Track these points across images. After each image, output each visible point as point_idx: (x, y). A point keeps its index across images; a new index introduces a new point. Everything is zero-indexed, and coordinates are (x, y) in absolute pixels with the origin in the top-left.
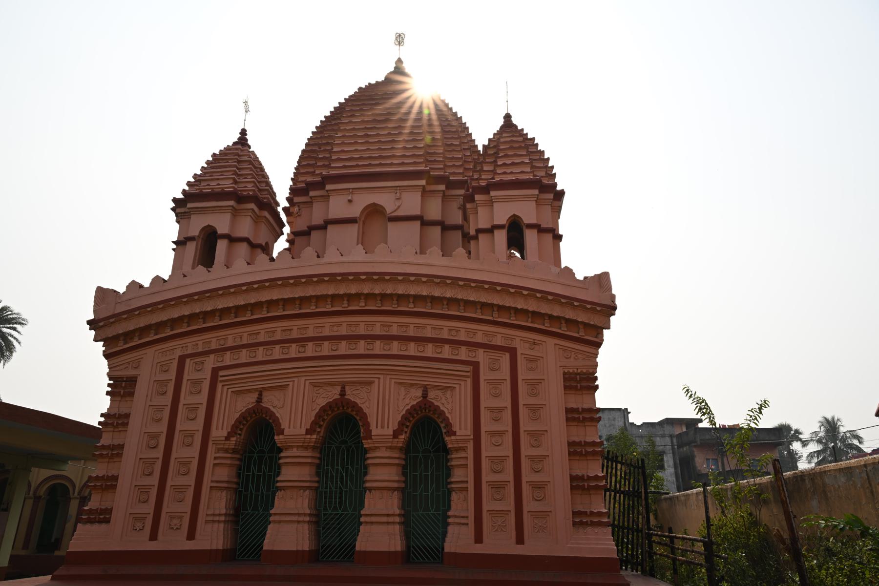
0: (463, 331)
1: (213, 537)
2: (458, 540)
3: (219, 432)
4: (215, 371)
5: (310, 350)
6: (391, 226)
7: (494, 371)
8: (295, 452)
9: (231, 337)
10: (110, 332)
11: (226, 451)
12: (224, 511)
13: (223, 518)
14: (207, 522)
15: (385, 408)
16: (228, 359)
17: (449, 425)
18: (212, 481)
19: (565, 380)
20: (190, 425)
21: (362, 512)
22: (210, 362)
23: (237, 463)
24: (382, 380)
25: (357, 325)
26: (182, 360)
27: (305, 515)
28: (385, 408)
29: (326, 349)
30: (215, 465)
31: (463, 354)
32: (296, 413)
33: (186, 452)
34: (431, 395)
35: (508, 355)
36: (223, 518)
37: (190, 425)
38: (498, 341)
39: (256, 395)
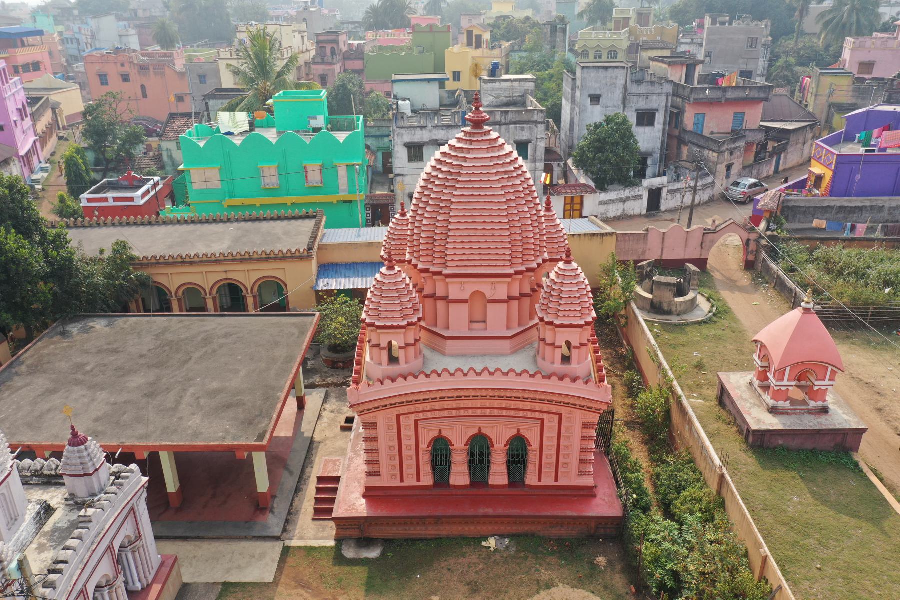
0: (538, 407)
1: (427, 480)
2: (531, 479)
3: (423, 446)
4: (416, 422)
5: (462, 413)
6: (489, 306)
7: (551, 423)
9: (421, 407)
15: (500, 436)
16: (421, 416)
17: (528, 441)
20: (409, 442)
22: (413, 417)
26: (398, 417)
28: (500, 436)
29: (470, 413)
31: (537, 415)
32: (459, 438)
33: (409, 453)
34: (521, 432)
37: (409, 442)
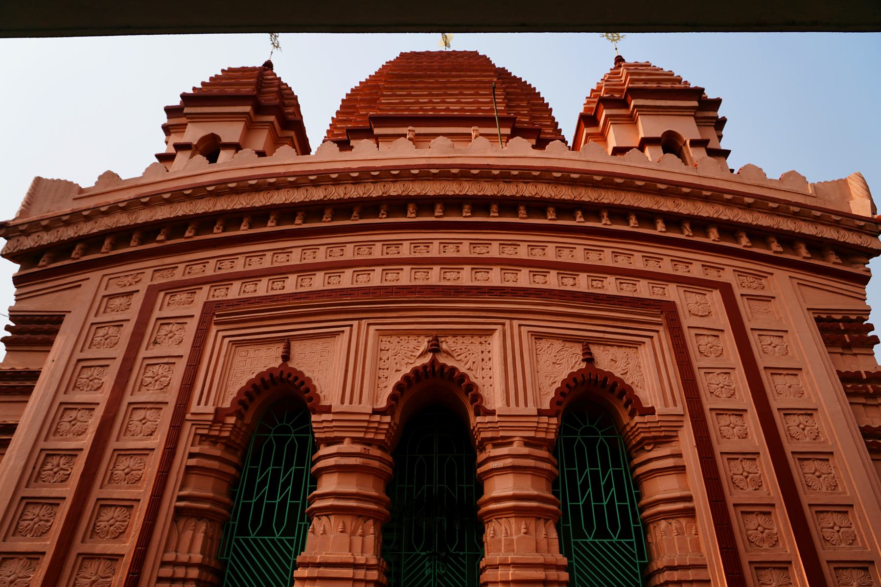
7: (701, 310)
8: (346, 447)
10: (28, 243)
11: (214, 440)
12: (197, 557)
13: (194, 573)
14: (160, 580)
18: (180, 498)
19: (822, 330)
21: (483, 564)
23: (232, 471)
24: (507, 327)
25: (458, 244)
27: (368, 567)
30: (188, 468)
35: (718, 292)
36: (194, 573)
38: (696, 271)
39: (277, 350)
